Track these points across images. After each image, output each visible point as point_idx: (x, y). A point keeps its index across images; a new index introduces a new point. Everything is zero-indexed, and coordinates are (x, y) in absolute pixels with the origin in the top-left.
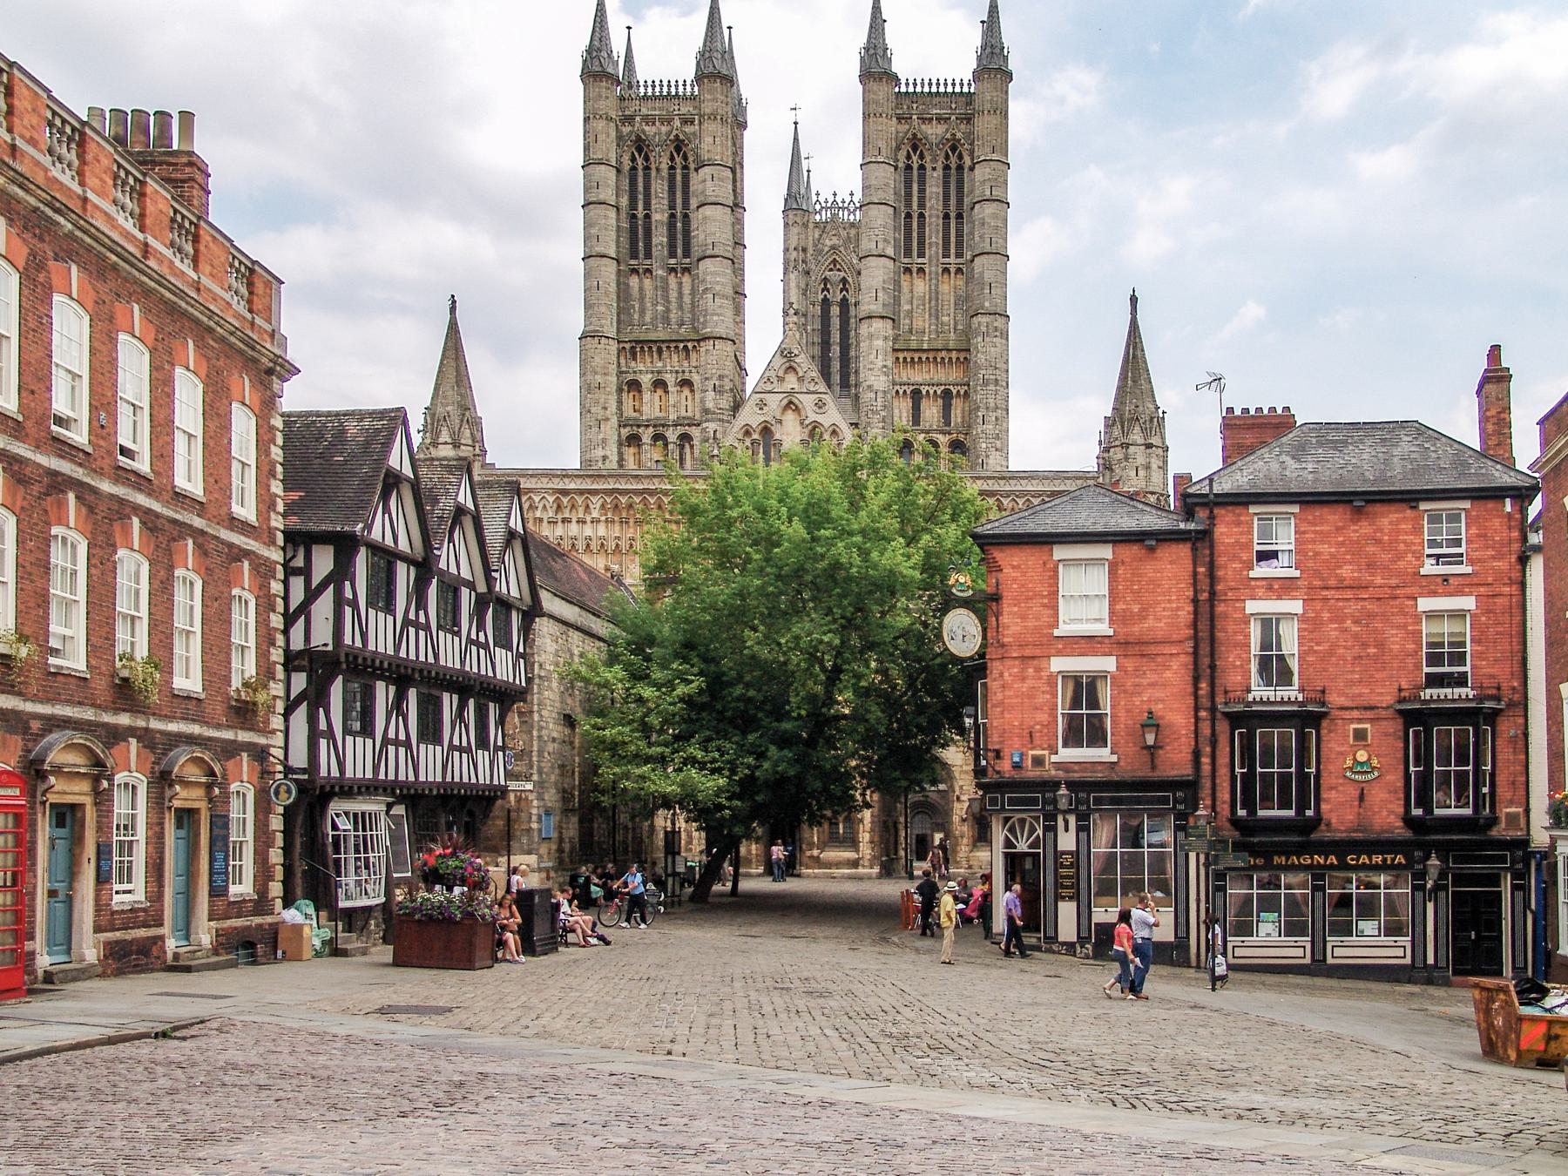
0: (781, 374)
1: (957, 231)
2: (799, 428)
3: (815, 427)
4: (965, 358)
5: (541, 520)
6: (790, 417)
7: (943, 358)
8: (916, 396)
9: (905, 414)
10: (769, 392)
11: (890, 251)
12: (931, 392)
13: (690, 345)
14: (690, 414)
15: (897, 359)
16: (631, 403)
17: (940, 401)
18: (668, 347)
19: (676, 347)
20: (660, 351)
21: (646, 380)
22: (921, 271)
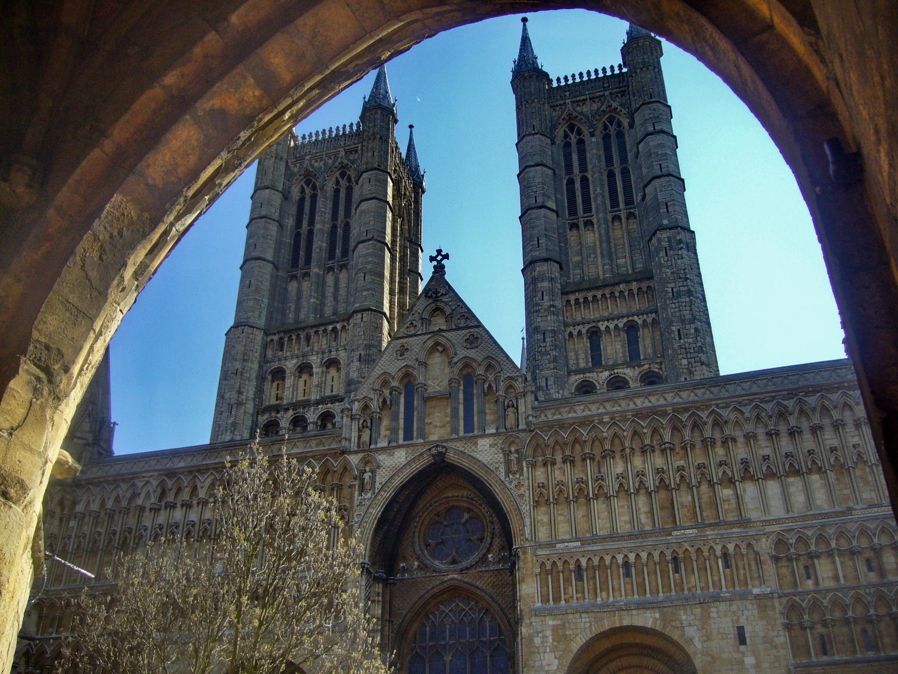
0: (426, 316)
1: (624, 182)
2: (447, 370)
3: (467, 366)
4: (649, 287)
5: (142, 509)
6: (437, 360)
7: (621, 292)
8: (595, 335)
9: (582, 356)
10: (411, 336)
11: (552, 204)
12: (612, 326)
13: (339, 326)
14: (333, 393)
15: (568, 301)
16: (274, 392)
17: (624, 335)
18: (316, 332)
19: (325, 331)
20: (308, 338)
21: (290, 365)
22: (589, 223)
